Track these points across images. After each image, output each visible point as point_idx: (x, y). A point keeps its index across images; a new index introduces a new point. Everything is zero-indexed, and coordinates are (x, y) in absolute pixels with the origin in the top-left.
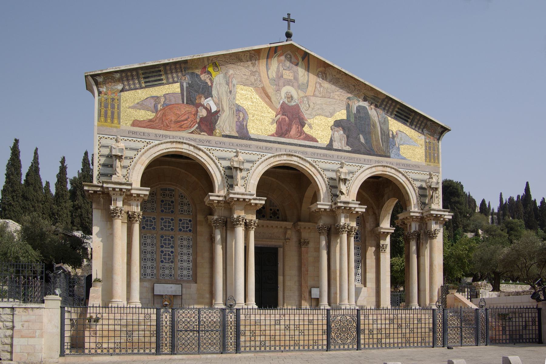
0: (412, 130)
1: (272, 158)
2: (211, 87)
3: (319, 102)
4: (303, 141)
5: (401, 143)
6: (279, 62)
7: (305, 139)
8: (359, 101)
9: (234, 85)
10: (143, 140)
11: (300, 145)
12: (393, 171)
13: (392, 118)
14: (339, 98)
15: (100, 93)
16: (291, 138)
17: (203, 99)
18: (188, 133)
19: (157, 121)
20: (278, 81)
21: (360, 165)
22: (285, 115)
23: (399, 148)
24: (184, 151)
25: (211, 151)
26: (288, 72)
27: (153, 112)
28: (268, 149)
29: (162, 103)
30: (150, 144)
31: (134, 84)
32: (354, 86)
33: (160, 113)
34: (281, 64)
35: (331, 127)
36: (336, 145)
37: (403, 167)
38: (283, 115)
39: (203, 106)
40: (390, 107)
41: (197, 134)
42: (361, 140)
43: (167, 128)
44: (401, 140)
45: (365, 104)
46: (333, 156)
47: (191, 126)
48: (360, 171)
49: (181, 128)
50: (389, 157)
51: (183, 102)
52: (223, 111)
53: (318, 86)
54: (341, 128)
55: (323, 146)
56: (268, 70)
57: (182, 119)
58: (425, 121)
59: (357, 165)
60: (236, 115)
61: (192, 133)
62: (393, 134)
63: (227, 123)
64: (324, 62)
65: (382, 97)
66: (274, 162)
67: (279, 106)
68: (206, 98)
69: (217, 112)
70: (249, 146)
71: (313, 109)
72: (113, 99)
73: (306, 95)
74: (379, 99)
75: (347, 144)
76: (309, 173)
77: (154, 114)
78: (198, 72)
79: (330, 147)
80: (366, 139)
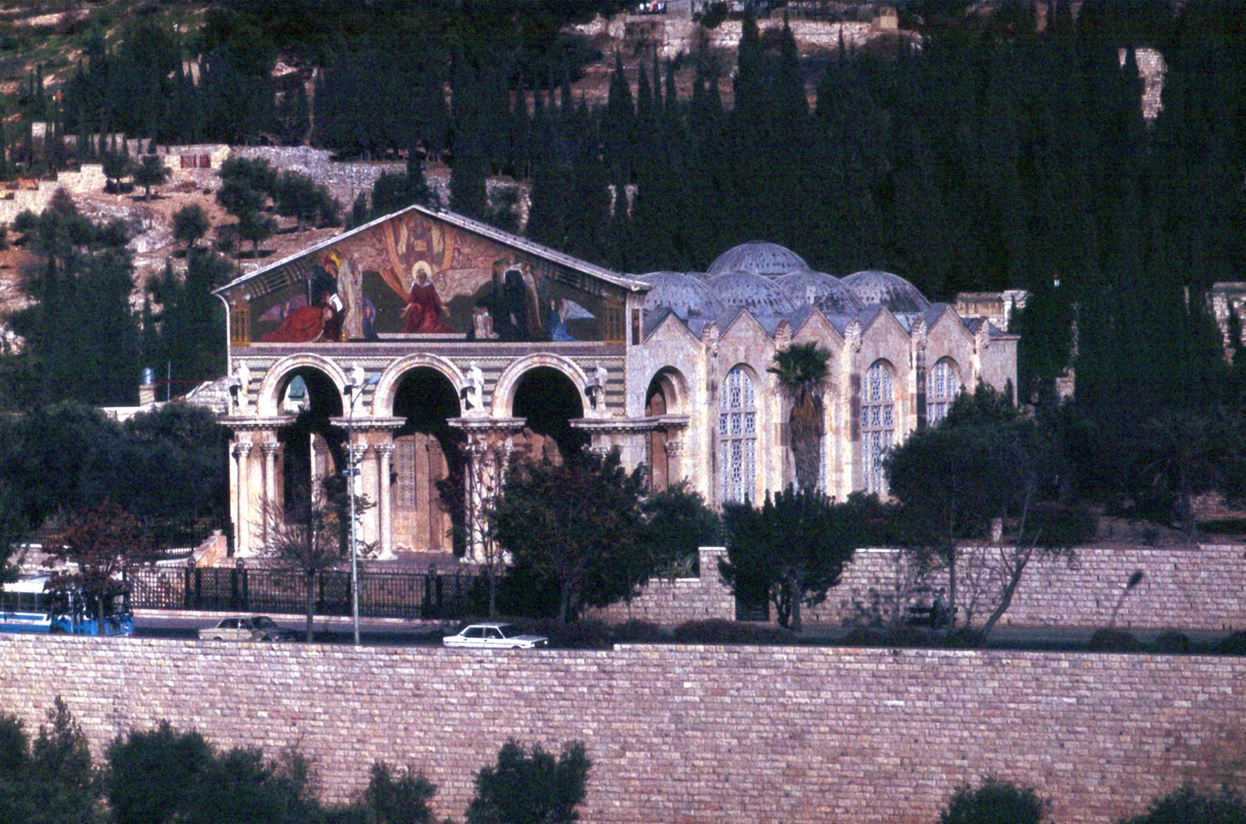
6: (409, 230)
8: (509, 264)
15: (231, 307)
20: (410, 257)
28: (399, 351)
36: (480, 333)
45: (518, 267)
49: (306, 338)
56: (397, 242)
67: (410, 291)
69: (343, 311)
70: (376, 350)
75: (495, 330)
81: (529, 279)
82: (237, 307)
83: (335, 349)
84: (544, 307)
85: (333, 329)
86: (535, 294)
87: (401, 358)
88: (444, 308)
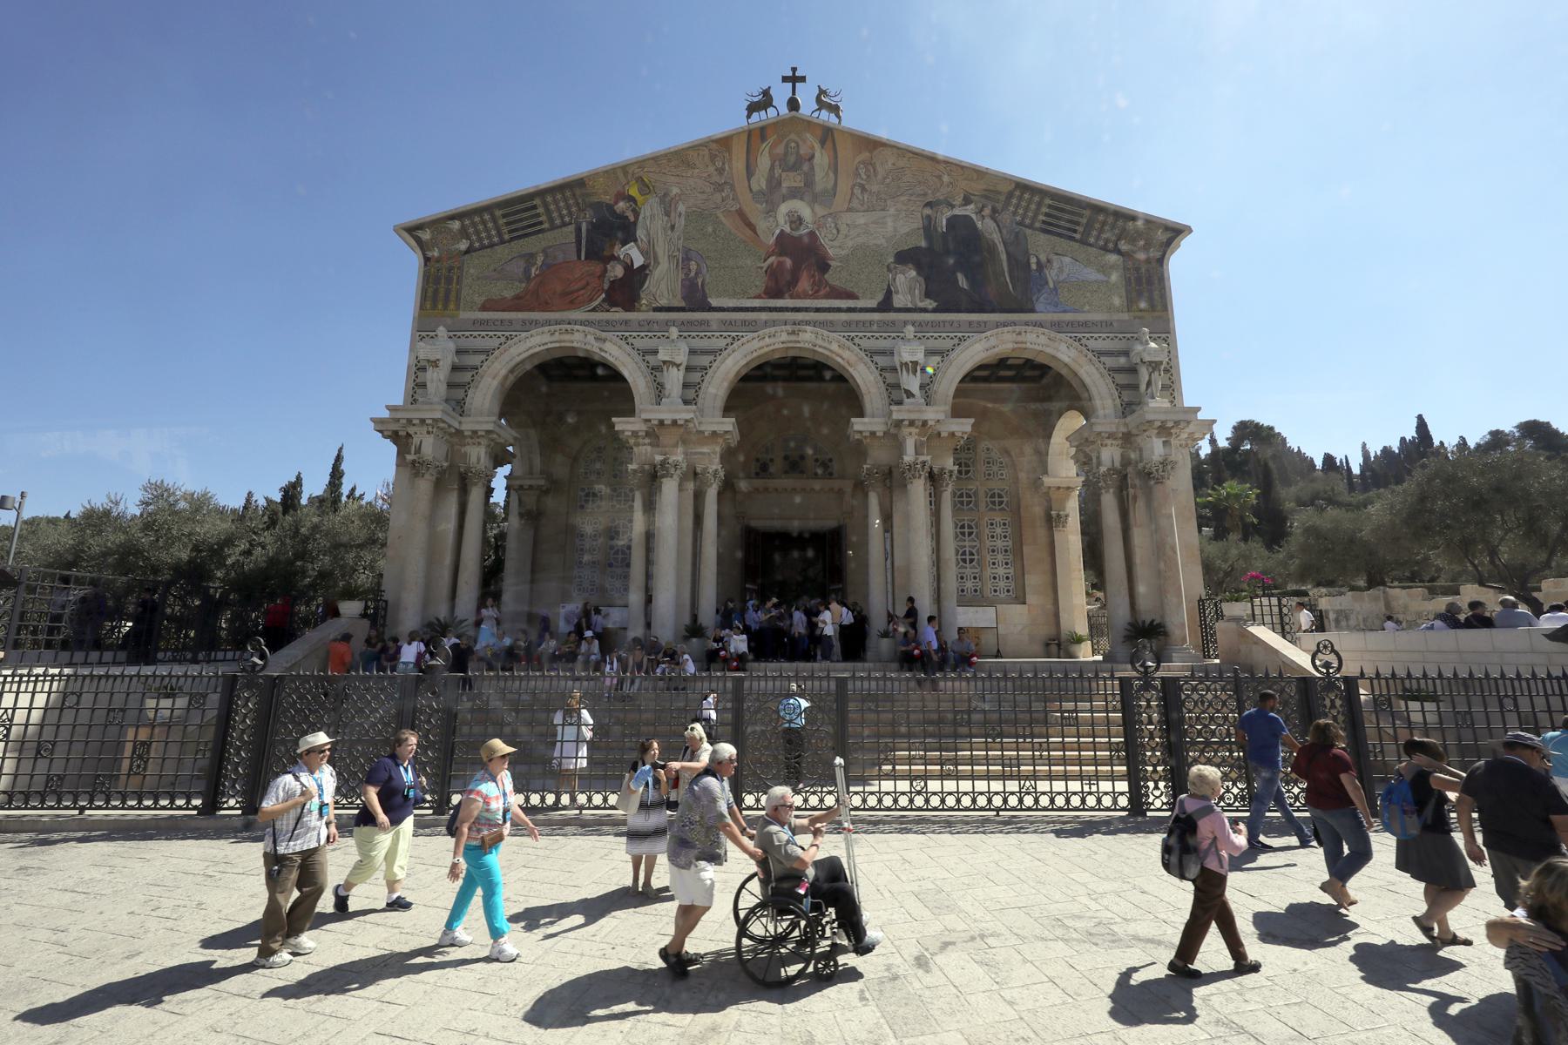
0: (1089, 248)
1: (755, 341)
2: (635, 223)
3: (862, 221)
4: (824, 301)
5: (1061, 278)
7: (827, 296)
8: (953, 206)
9: (680, 214)
10: (499, 334)
11: (818, 310)
12: (1043, 339)
13: (1037, 229)
14: (904, 208)
15: (427, 260)
16: (798, 297)
17: (616, 247)
21: (960, 335)
22: (786, 254)
23: (1055, 289)
24: (575, 345)
25: (630, 340)
26: (791, 174)
27: (521, 282)
28: (752, 326)
29: (539, 263)
31: (489, 237)
32: (937, 177)
34: (777, 163)
35: (888, 267)
36: (899, 300)
37: (1069, 329)
38: (781, 255)
40: (1027, 209)
42: (960, 283)
43: (545, 307)
44: (1061, 270)
46: (893, 323)
48: (958, 350)
49: (573, 304)
50: (1032, 311)
51: (579, 257)
53: (857, 191)
54: (911, 266)
55: (869, 306)
56: (750, 172)
57: (576, 287)
59: (952, 335)
61: (594, 310)
62: (1039, 263)
63: (663, 286)
65: (1006, 188)
66: (760, 348)
67: (772, 240)
68: (624, 243)
69: (643, 267)
71: (846, 236)
72: (450, 269)
73: (831, 211)
74: (999, 193)
75: (928, 295)
76: (839, 363)
77: (524, 285)
78: (607, 199)
79: (886, 305)
81: (986, 226)
82: (438, 260)
83: (626, 322)
84: (1019, 263)
85: (626, 291)
86: (1001, 248)
87: (751, 335)
88: (832, 263)
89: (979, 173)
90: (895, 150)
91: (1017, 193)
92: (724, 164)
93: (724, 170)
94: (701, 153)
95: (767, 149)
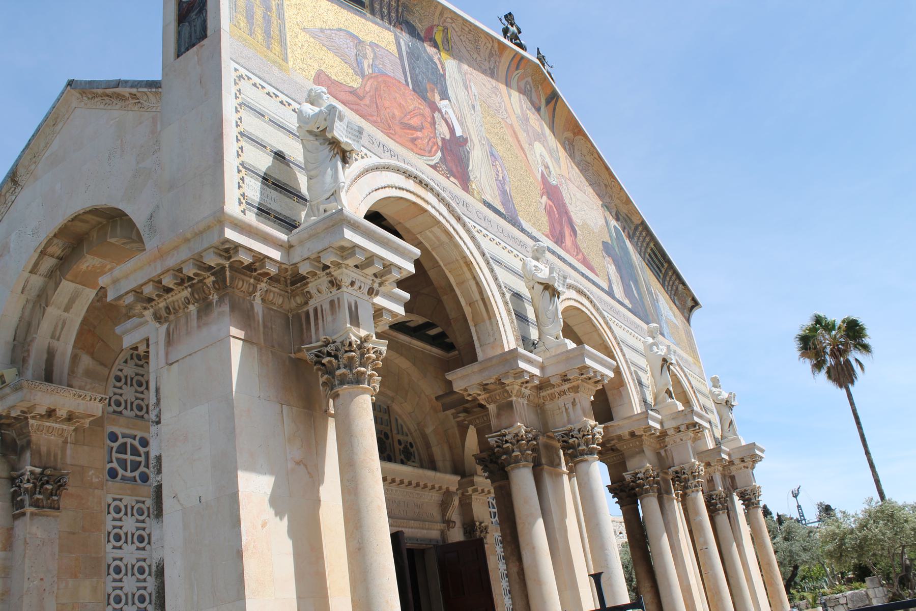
11: (583, 275)
18: (429, 165)
19: (367, 101)
30: (362, 157)
32: (606, 185)
33: (369, 83)
39: (440, 111)
41: (443, 175)
47: (430, 152)
52: (472, 144)
58: (677, 282)
60: (493, 165)
64: (577, 121)
65: (637, 221)
74: (632, 222)
80: (638, 293)
89: (628, 201)
90: (589, 146)
91: (640, 228)
92: (494, 67)
93: (494, 73)
94: (487, 44)
95: (517, 77)
